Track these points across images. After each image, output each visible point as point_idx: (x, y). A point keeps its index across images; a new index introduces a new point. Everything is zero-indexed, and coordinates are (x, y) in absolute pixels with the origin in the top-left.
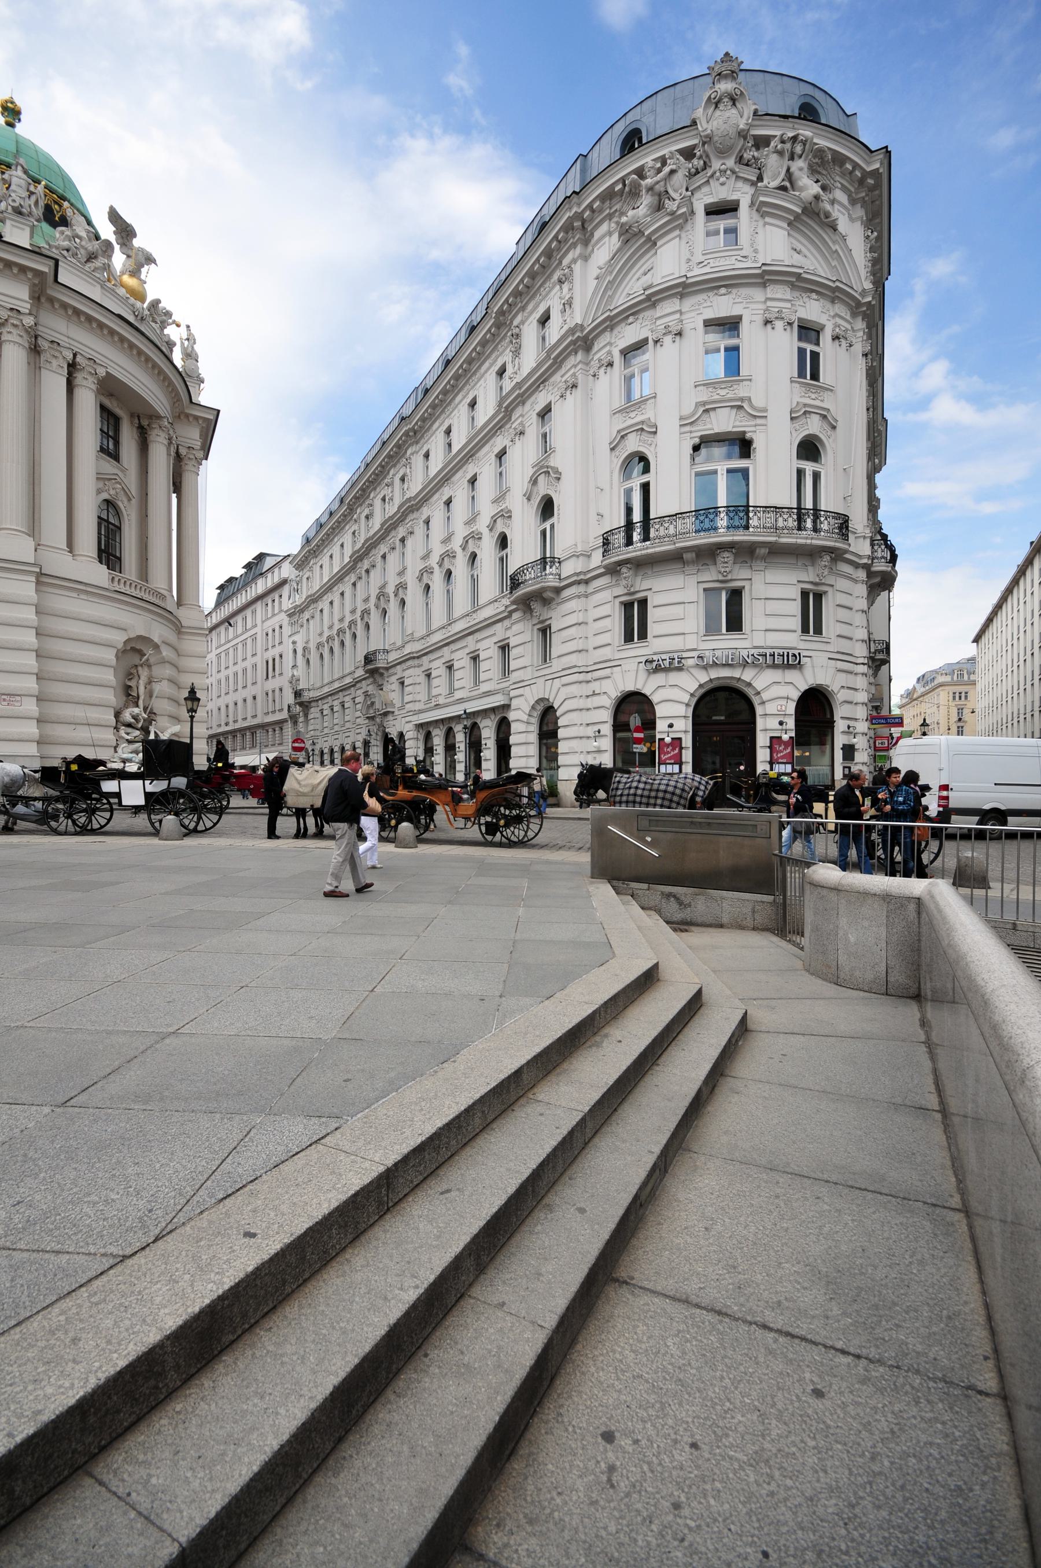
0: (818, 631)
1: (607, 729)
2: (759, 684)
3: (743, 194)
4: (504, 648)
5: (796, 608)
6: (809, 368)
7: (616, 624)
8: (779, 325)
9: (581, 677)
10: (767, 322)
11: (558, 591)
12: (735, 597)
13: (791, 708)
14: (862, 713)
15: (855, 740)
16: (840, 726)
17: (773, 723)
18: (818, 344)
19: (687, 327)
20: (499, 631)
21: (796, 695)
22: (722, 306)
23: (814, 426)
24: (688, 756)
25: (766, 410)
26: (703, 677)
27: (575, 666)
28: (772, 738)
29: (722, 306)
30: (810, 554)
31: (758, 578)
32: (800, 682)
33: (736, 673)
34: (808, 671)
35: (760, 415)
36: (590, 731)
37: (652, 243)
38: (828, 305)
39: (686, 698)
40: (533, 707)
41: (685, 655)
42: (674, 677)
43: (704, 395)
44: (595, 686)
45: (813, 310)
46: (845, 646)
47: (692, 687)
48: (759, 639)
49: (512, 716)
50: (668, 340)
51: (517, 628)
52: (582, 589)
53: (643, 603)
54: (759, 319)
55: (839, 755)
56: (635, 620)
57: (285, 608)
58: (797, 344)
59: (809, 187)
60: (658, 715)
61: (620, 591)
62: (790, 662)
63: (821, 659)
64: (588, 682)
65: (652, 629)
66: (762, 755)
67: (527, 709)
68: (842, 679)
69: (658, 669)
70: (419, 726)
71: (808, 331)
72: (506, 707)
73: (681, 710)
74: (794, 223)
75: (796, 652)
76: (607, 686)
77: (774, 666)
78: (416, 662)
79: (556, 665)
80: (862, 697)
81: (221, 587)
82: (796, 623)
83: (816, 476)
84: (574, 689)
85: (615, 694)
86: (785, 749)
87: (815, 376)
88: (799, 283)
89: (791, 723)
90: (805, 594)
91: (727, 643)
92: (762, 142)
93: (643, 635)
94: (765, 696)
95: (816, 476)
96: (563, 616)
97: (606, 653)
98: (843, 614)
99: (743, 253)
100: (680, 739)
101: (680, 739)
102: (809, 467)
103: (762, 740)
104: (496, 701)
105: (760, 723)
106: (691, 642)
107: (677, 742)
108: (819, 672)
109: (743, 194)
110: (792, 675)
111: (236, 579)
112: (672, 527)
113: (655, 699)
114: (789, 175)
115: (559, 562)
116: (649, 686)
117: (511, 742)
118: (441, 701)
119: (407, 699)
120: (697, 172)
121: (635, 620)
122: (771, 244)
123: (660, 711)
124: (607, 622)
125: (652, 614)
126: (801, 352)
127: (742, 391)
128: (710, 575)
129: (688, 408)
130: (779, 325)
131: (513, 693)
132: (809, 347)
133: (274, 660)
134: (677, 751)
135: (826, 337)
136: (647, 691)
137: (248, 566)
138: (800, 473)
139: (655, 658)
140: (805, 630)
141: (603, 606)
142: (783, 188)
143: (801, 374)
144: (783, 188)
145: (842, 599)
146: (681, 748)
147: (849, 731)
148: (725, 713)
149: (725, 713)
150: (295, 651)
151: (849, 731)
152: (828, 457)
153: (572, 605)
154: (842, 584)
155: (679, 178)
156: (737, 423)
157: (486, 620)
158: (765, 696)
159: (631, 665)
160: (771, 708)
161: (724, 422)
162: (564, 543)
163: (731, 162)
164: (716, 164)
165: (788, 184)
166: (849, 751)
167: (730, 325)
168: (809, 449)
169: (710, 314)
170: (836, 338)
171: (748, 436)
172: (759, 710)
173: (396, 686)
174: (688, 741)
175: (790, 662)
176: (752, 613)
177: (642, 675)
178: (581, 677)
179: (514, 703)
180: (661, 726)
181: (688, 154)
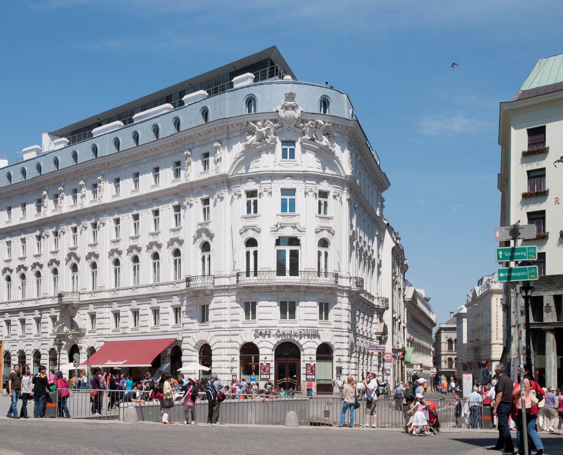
1: (237, 358)
8: (311, 194)
10: (306, 193)
13: (314, 352)
14: (346, 353)
15: (341, 365)
16: (335, 359)
21: (316, 346)
22: (288, 184)
24: (272, 371)
26: (280, 339)
28: (307, 364)
29: (288, 184)
36: (229, 358)
46: (338, 325)
49: (183, 346)
60: (260, 353)
63: (327, 331)
65: (258, 316)
66: (303, 371)
67: (194, 344)
71: (323, 194)
75: (316, 329)
79: (212, 325)
80: (346, 346)
82: (317, 316)
83: (326, 254)
85: (241, 343)
88: (319, 178)
89: (314, 358)
93: (254, 317)
95: (326, 254)
99: (297, 163)
101: (269, 364)
102: (323, 250)
103: (303, 365)
105: (302, 358)
108: (326, 337)
112: (267, 276)
113: (259, 346)
115: (214, 278)
117: (182, 360)
118: (128, 331)
119: (97, 326)
122: (308, 162)
123: (261, 351)
130: (311, 194)
135: (330, 196)
138: (319, 253)
139: (259, 329)
140: (321, 318)
148: (288, 352)
149: (288, 352)
156: (294, 233)
160: (306, 352)
161: (289, 232)
166: (340, 370)
167: (292, 192)
168: (324, 243)
169: (283, 186)
171: (298, 238)
172: (302, 353)
174: (273, 365)
179: (185, 340)
180: (261, 358)
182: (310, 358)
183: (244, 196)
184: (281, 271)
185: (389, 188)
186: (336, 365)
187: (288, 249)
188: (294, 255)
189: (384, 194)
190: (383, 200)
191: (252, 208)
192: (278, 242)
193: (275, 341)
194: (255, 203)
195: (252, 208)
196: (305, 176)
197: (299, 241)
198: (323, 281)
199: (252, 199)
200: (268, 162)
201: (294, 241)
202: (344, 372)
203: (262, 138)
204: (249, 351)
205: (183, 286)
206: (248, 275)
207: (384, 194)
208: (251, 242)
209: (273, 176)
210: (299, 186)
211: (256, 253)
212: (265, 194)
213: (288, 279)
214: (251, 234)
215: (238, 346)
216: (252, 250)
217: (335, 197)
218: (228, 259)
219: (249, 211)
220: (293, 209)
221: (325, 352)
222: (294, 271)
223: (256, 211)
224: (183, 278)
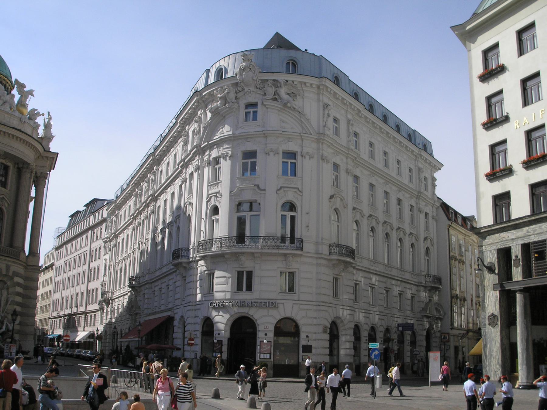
18: (295, 159)
25: (265, 190)
27: (190, 302)
41: (225, 301)
57: (103, 237)
62: (271, 305)
64: (195, 310)
75: (273, 301)
81: (72, 216)
86: (267, 347)
91: (245, 296)
92: (264, 81)
95: (293, 218)
100: (222, 341)
101: (222, 341)
102: (289, 214)
108: (288, 309)
110: (272, 312)
111: (80, 212)
120: (240, 92)
130: (272, 154)
133: (94, 269)
134: (220, 346)
135: (299, 157)
137: (87, 205)
138: (284, 217)
146: (222, 345)
148: (243, 328)
149: (243, 328)
150: (106, 266)
157: (165, 273)
163: (252, 89)
164: (246, 89)
165: (277, 97)
174: (225, 342)
175: (271, 305)
178: (193, 308)
182: (266, 335)
189: (437, 175)
207: (437, 175)
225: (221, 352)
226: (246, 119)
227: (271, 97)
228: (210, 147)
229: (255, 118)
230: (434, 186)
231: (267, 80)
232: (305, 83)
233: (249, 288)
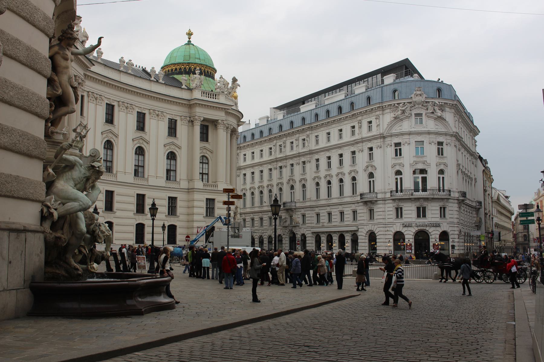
0: (444, 216)
1: (392, 240)
2: (430, 231)
3: (423, 112)
4: (355, 212)
5: (439, 212)
6: (440, 152)
7: (394, 213)
8: (433, 144)
9: (384, 226)
11: (376, 201)
12: (424, 209)
13: (438, 236)
14: (456, 236)
16: (451, 240)
17: (434, 240)
19: (411, 142)
20: (353, 207)
21: (439, 233)
22: (419, 138)
23: (442, 167)
24: (413, 248)
26: (417, 229)
29: (419, 138)
30: (442, 199)
31: (429, 205)
32: (440, 230)
33: (425, 228)
34: (442, 227)
35: (429, 165)
36: (387, 240)
37: (402, 120)
38: (444, 136)
39: (413, 234)
40: (367, 232)
42: (410, 229)
43: (415, 159)
44: (388, 229)
45: (441, 139)
46: (451, 220)
47: (414, 231)
48: (430, 220)
49: (359, 234)
50: (406, 144)
51: (360, 208)
52: (384, 202)
53: (401, 208)
54: (428, 142)
55: (450, 248)
56: (399, 212)
58: (437, 147)
59: (439, 113)
61: (395, 205)
62: (437, 225)
63: (445, 224)
65: (404, 216)
68: (451, 229)
69: (405, 226)
70: (313, 233)
71: (440, 143)
72: (357, 231)
73: (411, 237)
74: (435, 119)
76: (391, 229)
77: (433, 226)
78: (312, 209)
79: (375, 221)
80: (457, 232)
82: (439, 216)
83: (443, 178)
84: (382, 229)
85: (394, 232)
87: (442, 155)
88: (437, 134)
89: (438, 240)
90: (441, 208)
91: (422, 220)
92: (426, 102)
93: (401, 217)
94: (432, 234)
95: (443, 178)
96: (378, 208)
97: (391, 220)
98: (451, 212)
102: (441, 176)
103: (431, 244)
104: (354, 228)
106: (414, 220)
107: (411, 244)
108: (445, 227)
109: (423, 112)
110: (438, 228)
113: (405, 234)
114: (434, 109)
116: (403, 230)
118: (325, 224)
121: (399, 212)
122: (430, 125)
123: (406, 237)
124: (391, 213)
125: (404, 212)
126: (438, 148)
127: (424, 159)
128: (418, 204)
129: (412, 162)
131: (359, 227)
132: (440, 147)
135: (444, 144)
136: (403, 231)
138: (439, 178)
141: (390, 208)
142: (433, 113)
143: (439, 154)
144: (433, 113)
145: (450, 208)
147: (453, 241)
148: (422, 238)
149: (422, 238)
151: (453, 241)
152: (446, 174)
153: (381, 206)
154: (450, 205)
155: (408, 109)
158: (432, 234)
159: (398, 225)
160: (433, 236)
161: (420, 166)
162: (379, 187)
163: (420, 106)
164: (417, 106)
166: (453, 247)
168: (441, 172)
170: (447, 144)
172: (430, 237)
173: (300, 216)
174: (413, 244)
175: (437, 225)
176: (428, 213)
177: (401, 227)
178: (384, 226)
179: (360, 230)
180: (406, 240)
181: (410, 103)
183: (393, 145)
184: (416, 190)
185: (480, 134)
186: (451, 244)
187: (421, 176)
188: (424, 180)
190: (476, 142)
191: (398, 153)
192: (414, 172)
193: (414, 230)
194: (400, 150)
195: (398, 153)
196: (429, 133)
197: (427, 171)
198: (442, 194)
199: (398, 148)
200: (406, 126)
201: (423, 171)
202: (456, 248)
203: (403, 112)
204: (398, 237)
205: (358, 198)
206: (397, 192)
207: (476, 138)
208: (399, 173)
209: (410, 134)
210: (425, 139)
211: (401, 179)
212: (406, 144)
213: (420, 194)
214: (398, 168)
215: (392, 234)
216: (399, 177)
217: (447, 144)
218: (384, 183)
219: (396, 155)
220: (423, 152)
221: (444, 236)
222: (424, 190)
223: (400, 155)
224: (358, 193)
225: (411, 250)
226: (416, 123)
227: (431, 111)
228: (391, 136)
229: (421, 122)
230: (476, 146)
231: (429, 102)
232: (447, 103)
233: (424, 216)
